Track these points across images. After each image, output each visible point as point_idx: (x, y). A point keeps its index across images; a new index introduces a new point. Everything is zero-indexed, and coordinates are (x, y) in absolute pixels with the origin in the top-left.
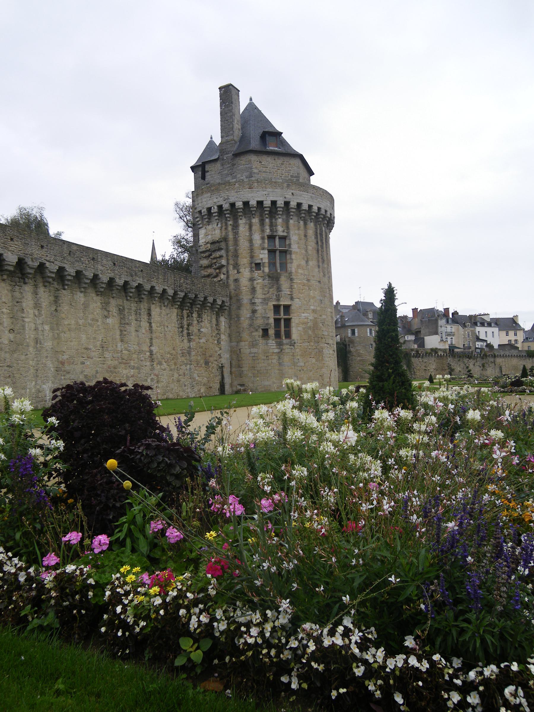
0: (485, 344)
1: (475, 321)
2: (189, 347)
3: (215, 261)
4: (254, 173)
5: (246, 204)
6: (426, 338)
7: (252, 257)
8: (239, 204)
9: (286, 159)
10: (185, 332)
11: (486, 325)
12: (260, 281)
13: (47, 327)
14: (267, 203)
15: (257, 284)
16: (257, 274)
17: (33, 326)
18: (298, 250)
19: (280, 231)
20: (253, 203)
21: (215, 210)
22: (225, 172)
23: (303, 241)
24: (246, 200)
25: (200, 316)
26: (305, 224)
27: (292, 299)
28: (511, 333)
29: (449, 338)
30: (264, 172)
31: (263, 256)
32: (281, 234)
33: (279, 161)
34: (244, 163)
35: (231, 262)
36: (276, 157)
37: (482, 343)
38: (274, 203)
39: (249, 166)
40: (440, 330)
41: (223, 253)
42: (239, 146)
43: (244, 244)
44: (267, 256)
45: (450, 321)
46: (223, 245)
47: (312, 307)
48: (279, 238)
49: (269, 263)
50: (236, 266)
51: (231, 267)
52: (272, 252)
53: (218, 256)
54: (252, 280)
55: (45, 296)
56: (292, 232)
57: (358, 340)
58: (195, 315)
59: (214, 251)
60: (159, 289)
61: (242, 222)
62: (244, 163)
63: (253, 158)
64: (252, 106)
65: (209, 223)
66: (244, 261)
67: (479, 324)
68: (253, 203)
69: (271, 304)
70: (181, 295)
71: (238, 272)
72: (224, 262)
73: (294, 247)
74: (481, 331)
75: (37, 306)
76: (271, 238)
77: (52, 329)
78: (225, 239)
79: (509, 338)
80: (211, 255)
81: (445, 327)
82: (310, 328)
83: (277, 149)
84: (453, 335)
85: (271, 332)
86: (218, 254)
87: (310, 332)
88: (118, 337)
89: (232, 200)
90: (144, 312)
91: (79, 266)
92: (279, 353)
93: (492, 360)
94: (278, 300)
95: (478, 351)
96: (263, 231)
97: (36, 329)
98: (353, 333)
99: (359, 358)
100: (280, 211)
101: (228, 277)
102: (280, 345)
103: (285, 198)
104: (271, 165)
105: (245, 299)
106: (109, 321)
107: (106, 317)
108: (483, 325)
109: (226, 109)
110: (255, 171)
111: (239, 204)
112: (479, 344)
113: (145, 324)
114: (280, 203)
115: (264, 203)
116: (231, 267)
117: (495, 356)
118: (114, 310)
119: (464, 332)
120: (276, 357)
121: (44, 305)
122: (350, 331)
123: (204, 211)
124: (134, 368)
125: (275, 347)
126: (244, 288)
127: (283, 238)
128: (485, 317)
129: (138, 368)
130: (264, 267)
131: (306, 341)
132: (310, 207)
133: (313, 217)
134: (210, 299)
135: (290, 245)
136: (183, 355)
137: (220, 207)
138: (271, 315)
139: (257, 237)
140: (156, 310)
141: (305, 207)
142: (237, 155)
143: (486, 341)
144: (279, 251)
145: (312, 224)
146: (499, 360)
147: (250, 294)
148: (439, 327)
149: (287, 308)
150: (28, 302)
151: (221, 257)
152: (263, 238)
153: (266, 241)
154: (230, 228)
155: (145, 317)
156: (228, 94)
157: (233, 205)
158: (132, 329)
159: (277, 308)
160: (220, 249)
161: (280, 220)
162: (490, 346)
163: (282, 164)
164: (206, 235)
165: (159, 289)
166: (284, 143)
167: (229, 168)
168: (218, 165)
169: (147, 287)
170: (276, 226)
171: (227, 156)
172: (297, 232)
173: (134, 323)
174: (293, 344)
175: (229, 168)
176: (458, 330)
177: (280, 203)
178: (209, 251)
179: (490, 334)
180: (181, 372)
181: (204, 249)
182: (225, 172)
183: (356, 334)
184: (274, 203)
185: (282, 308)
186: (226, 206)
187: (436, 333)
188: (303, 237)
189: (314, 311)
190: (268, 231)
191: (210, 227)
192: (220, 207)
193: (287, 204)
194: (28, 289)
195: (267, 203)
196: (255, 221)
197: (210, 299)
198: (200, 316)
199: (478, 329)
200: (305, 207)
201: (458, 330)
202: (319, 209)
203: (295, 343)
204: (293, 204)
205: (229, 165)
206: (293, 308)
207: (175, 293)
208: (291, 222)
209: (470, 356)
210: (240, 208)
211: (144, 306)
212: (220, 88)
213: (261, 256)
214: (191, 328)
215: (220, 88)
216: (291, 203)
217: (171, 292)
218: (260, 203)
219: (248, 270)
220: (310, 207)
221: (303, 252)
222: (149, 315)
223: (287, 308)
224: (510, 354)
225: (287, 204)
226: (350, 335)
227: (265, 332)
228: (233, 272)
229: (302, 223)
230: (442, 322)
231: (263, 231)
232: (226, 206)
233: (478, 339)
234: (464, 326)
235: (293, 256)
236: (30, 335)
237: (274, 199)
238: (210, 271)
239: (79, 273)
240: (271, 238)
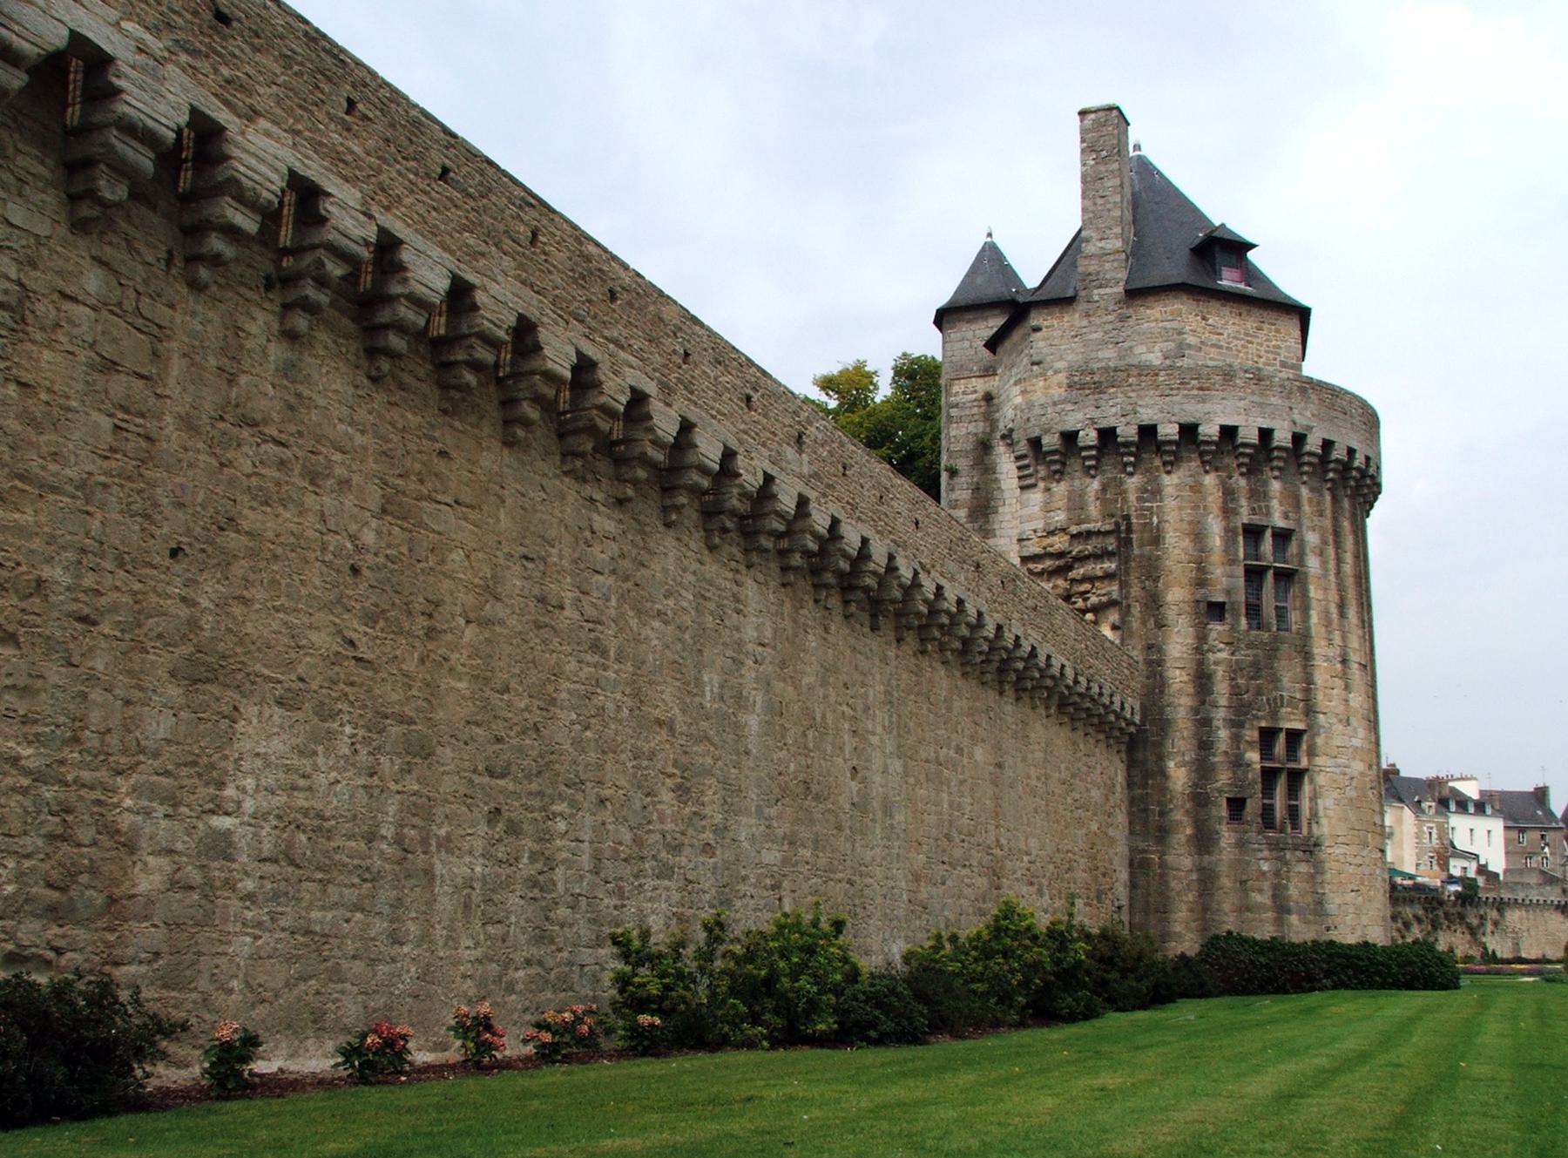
3: (1087, 586)
4: (1189, 346)
5: (1189, 431)
7: (1201, 582)
9: (1270, 316)
11: (1471, 810)
12: (1220, 655)
14: (1249, 435)
15: (1216, 663)
16: (1217, 629)
20: (1209, 430)
21: (1089, 437)
22: (1095, 336)
23: (1331, 551)
24: (1187, 419)
26: (1335, 500)
27: (1310, 711)
30: (1213, 345)
32: (1280, 523)
34: (1158, 315)
35: (1135, 591)
36: (1244, 309)
37: (1465, 864)
38: (1266, 434)
39: (1175, 325)
41: (1110, 566)
43: (1176, 547)
44: (1242, 581)
48: (1274, 535)
49: (1248, 605)
50: (1154, 603)
51: (1136, 609)
52: (1254, 575)
53: (1100, 574)
54: (1200, 647)
56: (1306, 523)
59: (1082, 559)
62: (1158, 315)
65: (1058, 475)
66: (1176, 595)
68: (1209, 430)
71: (1160, 625)
73: (1313, 563)
76: (1253, 533)
80: (1070, 568)
83: (1242, 286)
85: (1253, 807)
89: (1147, 415)
92: (1277, 873)
94: (1274, 715)
96: (1228, 512)
100: (1278, 458)
102: (1275, 846)
103: (1294, 423)
104: (1231, 329)
105: (1181, 704)
109: (1102, 168)
110: (1191, 340)
115: (1241, 432)
116: (1136, 609)
117: (1501, 906)
119: (1419, 828)
120: (1266, 885)
123: (1050, 441)
125: (1266, 853)
126: (1178, 672)
127: (1282, 537)
130: (1236, 617)
131: (1340, 840)
132: (1351, 452)
133: (1352, 483)
135: (1301, 555)
138: (1253, 756)
139: (1215, 527)
144: (1270, 571)
147: (1191, 690)
149: (1294, 737)
151: (1109, 576)
152: (1229, 533)
153: (1241, 539)
156: (1104, 129)
161: (1276, 486)
163: (1260, 329)
166: (1251, 274)
167: (1109, 327)
170: (1265, 496)
171: (1102, 291)
174: (1311, 848)
175: (1109, 327)
177: (1282, 437)
178: (1060, 555)
181: (1038, 550)
182: (1095, 336)
184: (1266, 434)
185: (1282, 738)
188: (1330, 539)
191: (1060, 489)
193: (1299, 439)
195: (1249, 435)
200: (1338, 453)
201: (1400, 821)
203: (1316, 845)
205: (1111, 318)
208: (1304, 492)
210: (1170, 442)
212: (1083, 113)
213: (1224, 582)
216: (1310, 439)
218: (1229, 432)
221: (1332, 578)
225: (1299, 439)
227: (1236, 805)
235: (1314, 592)
240: (1253, 533)
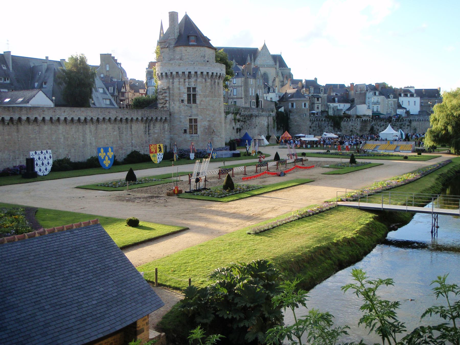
0: (405, 111)
2: (149, 139)
6: (357, 106)
8: (174, 73)
10: (147, 133)
13: (94, 138)
14: (187, 73)
17: (89, 139)
18: (201, 93)
19: (193, 85)
21: (164, 74)
25: (154, 125)
29: (375, 106)
31: (185, 97)
40: (367, 100)
41: (167, 94)
43: (176, 91)
45: (377, 93)
46: (168, 91)
47: (208, 119)
51: (171, 101)
55: (93, 127)
57: (295, 110)
58: (152, 125)
60: (135, 118)
61: (176, 80)
64: (187, 18)
67: (402, 95)
68: (180, 73)
69: (188, 118)
70: (145, 118)
72: (167, 99)
75: (91, 131)
77: (95, 139)
78: (169, 88)
81: (373, 98)
82: (206, 129)
85: (188, 131)
87: (206, 131)
88: (118, 139)
91: (104, 116)
97: (90, 139)
98: (292, 106)
99: (295, 124)
106: (115, 133)
107: (114, 132)
108: (406, 95)
110: (184, 55)
111: (174, 73)
112: (399, 111)
114: (193, 73)
121: (92, 131)
122: (290, 104)
124: (125, 150)
128: (410, 89)
129: (126, 150)
136: (146, 142)
138: (188, 122)
141: (205, 73)
142: (175, 47)
145: (209, 80)
148: (367, 99)
150: (88, 131)
154: (171, 83)
155: (129, 129)
159: (191, 120)
162: (408, 112)
165: (135, 118)
169: (130, 118)
172: (201, 85)
173: (125, 133)
180: (145, 150)
183: (295, 107)
184: (190, 73)
186: (169, 74)
187: (364, 103)
189: (209, 121)
190: (187, 86)
194: (87, 126)
196: (182, 80)
198: (154, 125)
200: (205, 73)
202: (212, 73)
204: (199, 73)
206: (198, 120)
207: (142, 118)
211: (129, 125)
212: (169, 13)
214: (150, 131)
215: (169, 13)
217: (140, 118)
218: (183, 73)
219: (178, 102)
220: (208, 73)
222: (131, 128)
223: (196, 120)
224: (424, 119)
225: (196, 73)
226: (290, 107)
227: (185, 131)
228: (172, 103)
229: (204, 80)
230: (370, 94)
231: (185, 85)
233: (400, 106)
237: (190, 71)
238: (163, 101)
239: (104, 118)
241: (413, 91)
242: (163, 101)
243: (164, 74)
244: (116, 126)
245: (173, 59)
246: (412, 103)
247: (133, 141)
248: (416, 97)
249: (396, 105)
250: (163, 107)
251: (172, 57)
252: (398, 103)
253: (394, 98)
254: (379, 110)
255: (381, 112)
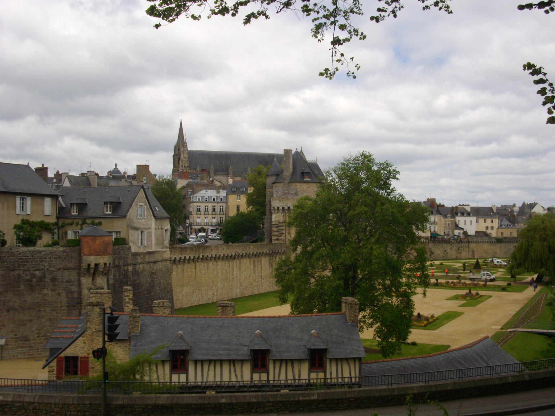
0: (462, 231)
1: (455, 212)
9: (312, 184)
21: (281, 208)
28: (489, 220)
29: (432, 227)
33: (309, 185)
35: (287, 231)
37: (459, 231)
42: (291, 178)
51: (287, 234)
60: (265, 252)
63: (298, 184)
65: (278, 213)
72: (284, 232)
74: (460, 220)
79: (486, 225)
84: (436, 224)
86: (282, 228)
90: (259, 261)
91: (246, 251)
93: (467, 245)
95: (456, 237)
101: (286, 238)
108: (463, 214)
112: (457, 232)
113: (260, 266)
116: (287, 234)
118: (252, 262)
119: (445, 222)
123: (276, 208)
128: (466, 208)
134: (280, 251)
137: (283, 208)
140: (263, 259)
142: (290, 182)
143: (463, 229)
146: (472, 245)
150: (235, 265)
151: (283, 229)
157: (289, 208)
158: (256, 268)
160: (282, 226)
162: (465, 233)
164: (276, 217)
165: (265, 252)
168: (282, 184)
176: (440, 220)
179: (468, 223)
186: (286, 208)
191: (278, 215)
192: (283, 208)
197: (280, 251)
199: (458, 218)
201: (440, 220)
209: (447, 242)
211: (260, 259)
217: (268, 252)
232: (286, 208)
233: (457, 227)
234: (445, 216)
236: (235, 275)
241: (469, 209)
242: (276, 233)
243: (281, 208)
244: (252, 260)
245: (288, 193)
246: (468, 223)
247: (262, 274)
248: (473, 216)
249: (454, 225)
250: (277, 239)
251: (286, 191)
252: (456, 222)
253: (451, 218)
254: (436, 231)
255: (439, 233)
